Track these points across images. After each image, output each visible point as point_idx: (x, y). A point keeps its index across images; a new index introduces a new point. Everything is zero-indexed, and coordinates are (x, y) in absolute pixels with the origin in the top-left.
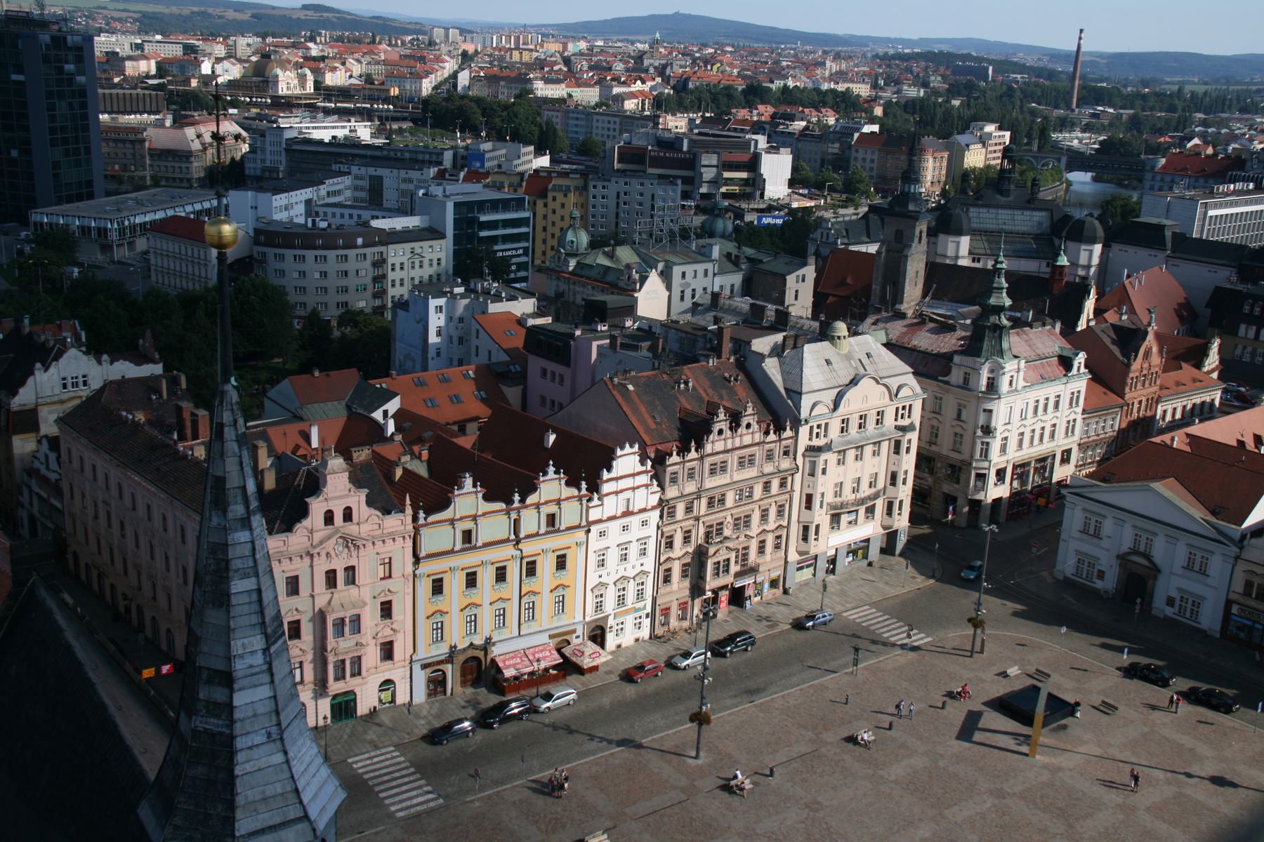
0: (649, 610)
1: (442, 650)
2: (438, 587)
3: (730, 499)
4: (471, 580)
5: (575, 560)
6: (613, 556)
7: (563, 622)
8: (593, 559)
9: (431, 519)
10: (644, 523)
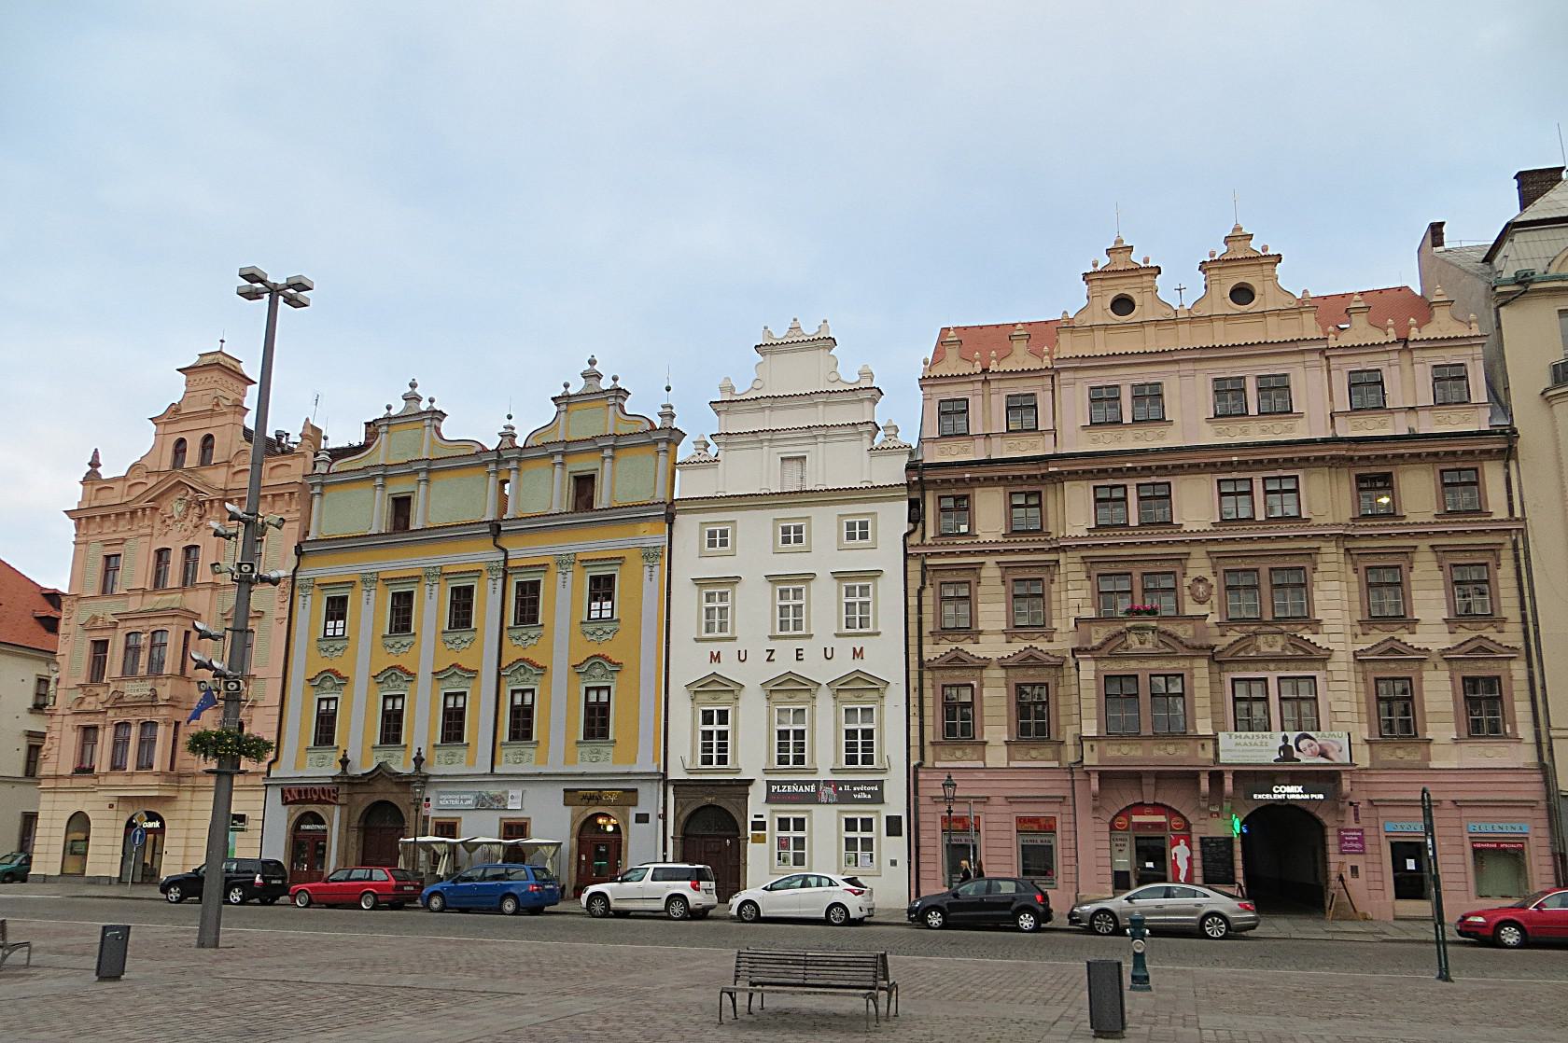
0: (896, 803)
1: (323, 768)
3: (1195, 504)
5: (636, 586)
6: (753, 611)
7: (602, 763)
8: (687, 606)
10: (857, 531)
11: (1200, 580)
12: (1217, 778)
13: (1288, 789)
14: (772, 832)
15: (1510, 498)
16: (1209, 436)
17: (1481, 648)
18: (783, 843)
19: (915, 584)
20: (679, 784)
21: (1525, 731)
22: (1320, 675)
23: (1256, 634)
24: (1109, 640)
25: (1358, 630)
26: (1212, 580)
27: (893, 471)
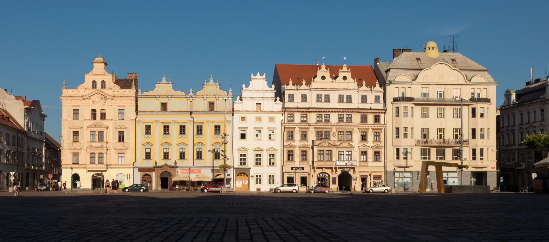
1: (149, 164)
2: (148, 129)
3: (334, 118)
4: (166, 129)
9: (144, 93)
10: (272, 119)
14: (255, 178)
18: (257, 180)
19: (283, 131)
20: (236, 169)
21: (383, 160)
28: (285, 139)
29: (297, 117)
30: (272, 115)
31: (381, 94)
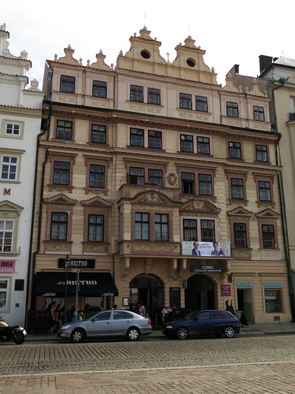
3: (171, 142)
11: (172, 175)
12: (180, 262)
13: (209, 267)
15: (277, 159)
16: (177, 115)
17: (268, 214)
22: (216, 220)
23: (193, 200)
24: (138, 195)
25: (228, 203)
26: (177, 176)
27: (36, 102)
28: (46, 182)
29: (82, 132)
30: (14, 119)
31: (265, 105)
